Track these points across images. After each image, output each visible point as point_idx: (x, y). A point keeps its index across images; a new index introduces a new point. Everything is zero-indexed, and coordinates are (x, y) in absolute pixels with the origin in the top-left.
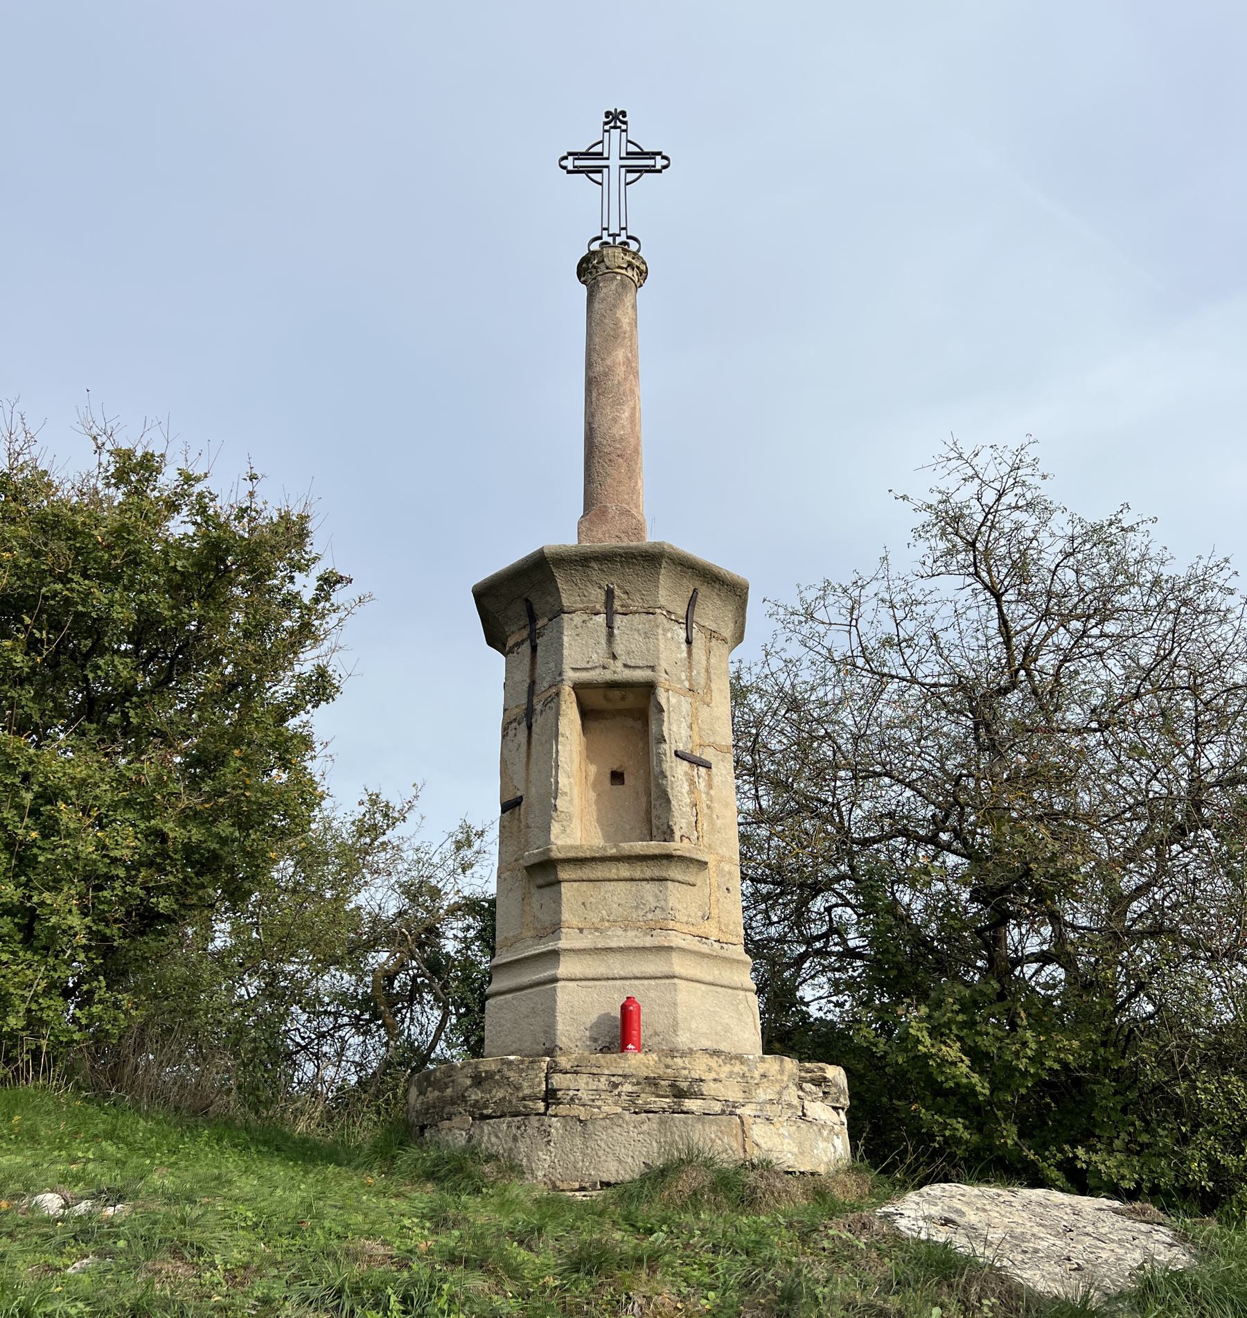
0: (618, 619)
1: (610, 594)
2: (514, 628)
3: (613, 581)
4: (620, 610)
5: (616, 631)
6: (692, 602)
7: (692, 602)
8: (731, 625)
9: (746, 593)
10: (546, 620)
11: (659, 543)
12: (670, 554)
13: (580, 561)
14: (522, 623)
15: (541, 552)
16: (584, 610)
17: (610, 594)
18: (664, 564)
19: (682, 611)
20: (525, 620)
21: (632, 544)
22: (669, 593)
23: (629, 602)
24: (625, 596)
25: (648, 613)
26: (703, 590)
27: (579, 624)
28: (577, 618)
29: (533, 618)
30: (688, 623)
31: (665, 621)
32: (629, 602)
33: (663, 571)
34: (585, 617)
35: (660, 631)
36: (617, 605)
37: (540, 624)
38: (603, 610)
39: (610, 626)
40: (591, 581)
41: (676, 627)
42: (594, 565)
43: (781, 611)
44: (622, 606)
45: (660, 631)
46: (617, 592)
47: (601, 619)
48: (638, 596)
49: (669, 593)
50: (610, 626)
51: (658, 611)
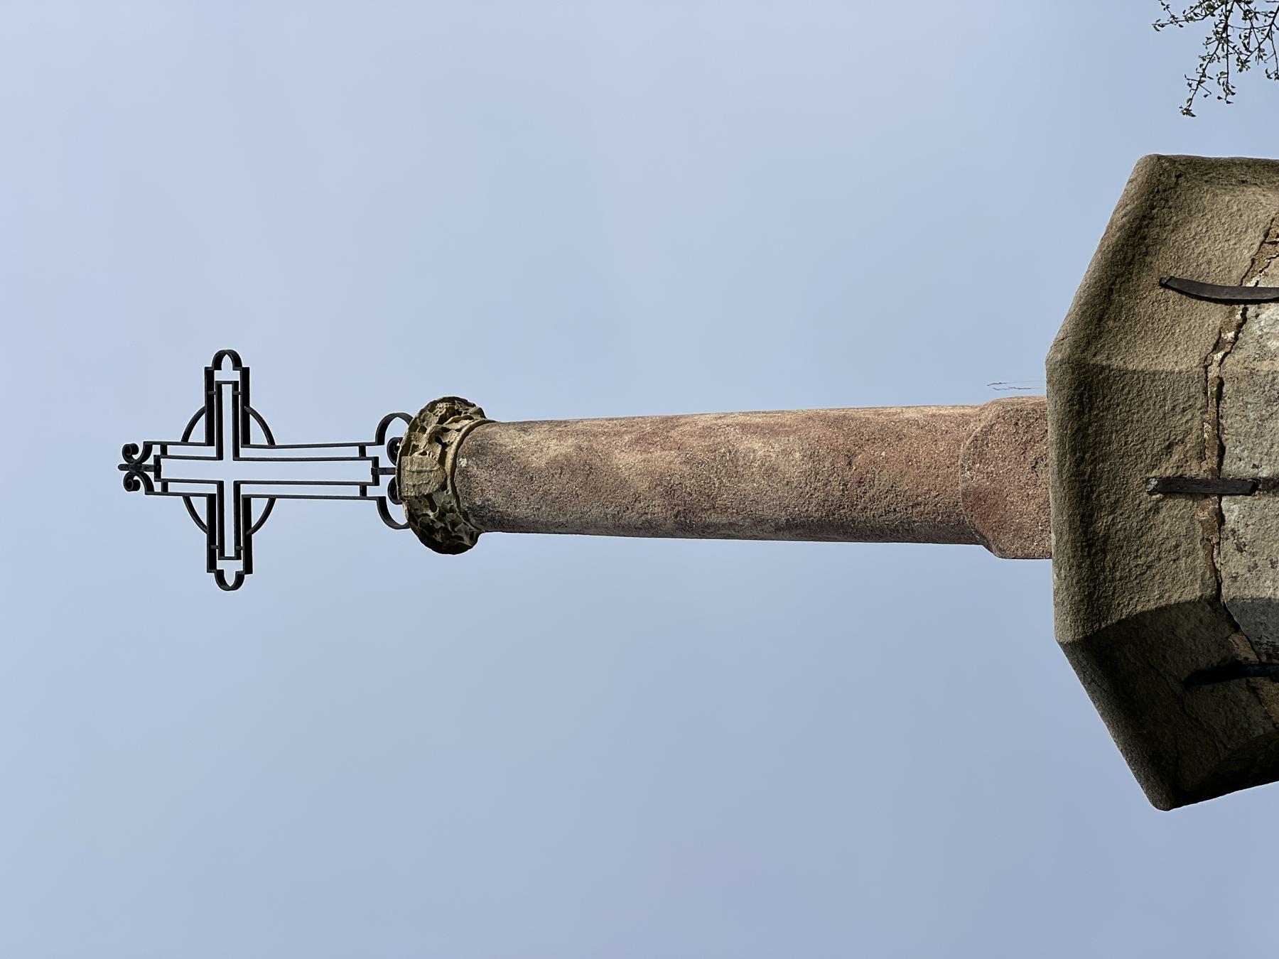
0: (1236, 466)
1: (1173, 487)
2: (1256, 714)
3: (1139, 481)
4: (1211, 462)
5: (1265, 473)
6: (1193, 290)
7: (1193, 290)
8: (1251, 193)
9: (1172, 160)
10: (1236, 638)
11: (1051, 372)
12: (1076, 346)
13: (1094, 560)
14: (1244, 695)
15: (1070, 648)
16: (1211, 548)
17: (1173, 487)
18: (1100, 359)
19: (1215, 315)
20: (1238, 689)
21: (1052, 436)
22: (1172, 347)
23: (1191, 440)
24: (1178, 449)
25: (1219, 396)
26: (1164, 264)
27: (1245, 559)
28: (1232, 564)
29: (1233, 669)
30: (1246, 299)
31: (1238, 355)
32: (1191, 440)
33: (1117, 362)
34: (1228, 546)
35: (1265, 366)
36: (1199, 470)
37: (1243, 651)
38: (1210, 504)
39: (1252, 487)
40: (1141, 532)
41: (1254, 328)
42: (1102, 523)
43: (1214, 69)
44: (1201, 457)
45: (1265, 366)
46: (1167, 469)
47: (1233, 508)
48: (1178, 421)
49: (1172, 347)
50: (1252, 487)
51: (1214, 371)
